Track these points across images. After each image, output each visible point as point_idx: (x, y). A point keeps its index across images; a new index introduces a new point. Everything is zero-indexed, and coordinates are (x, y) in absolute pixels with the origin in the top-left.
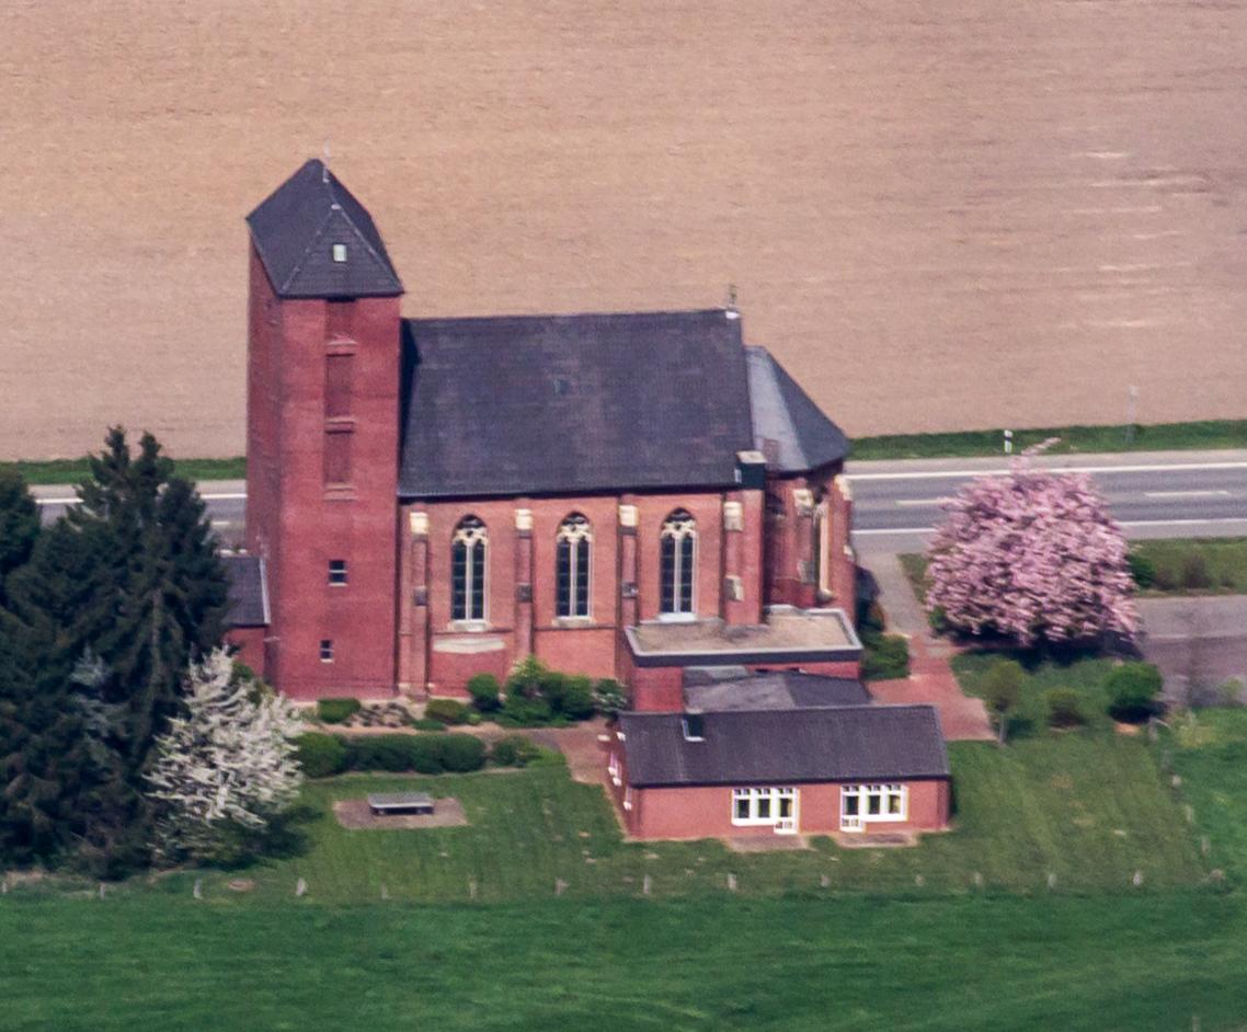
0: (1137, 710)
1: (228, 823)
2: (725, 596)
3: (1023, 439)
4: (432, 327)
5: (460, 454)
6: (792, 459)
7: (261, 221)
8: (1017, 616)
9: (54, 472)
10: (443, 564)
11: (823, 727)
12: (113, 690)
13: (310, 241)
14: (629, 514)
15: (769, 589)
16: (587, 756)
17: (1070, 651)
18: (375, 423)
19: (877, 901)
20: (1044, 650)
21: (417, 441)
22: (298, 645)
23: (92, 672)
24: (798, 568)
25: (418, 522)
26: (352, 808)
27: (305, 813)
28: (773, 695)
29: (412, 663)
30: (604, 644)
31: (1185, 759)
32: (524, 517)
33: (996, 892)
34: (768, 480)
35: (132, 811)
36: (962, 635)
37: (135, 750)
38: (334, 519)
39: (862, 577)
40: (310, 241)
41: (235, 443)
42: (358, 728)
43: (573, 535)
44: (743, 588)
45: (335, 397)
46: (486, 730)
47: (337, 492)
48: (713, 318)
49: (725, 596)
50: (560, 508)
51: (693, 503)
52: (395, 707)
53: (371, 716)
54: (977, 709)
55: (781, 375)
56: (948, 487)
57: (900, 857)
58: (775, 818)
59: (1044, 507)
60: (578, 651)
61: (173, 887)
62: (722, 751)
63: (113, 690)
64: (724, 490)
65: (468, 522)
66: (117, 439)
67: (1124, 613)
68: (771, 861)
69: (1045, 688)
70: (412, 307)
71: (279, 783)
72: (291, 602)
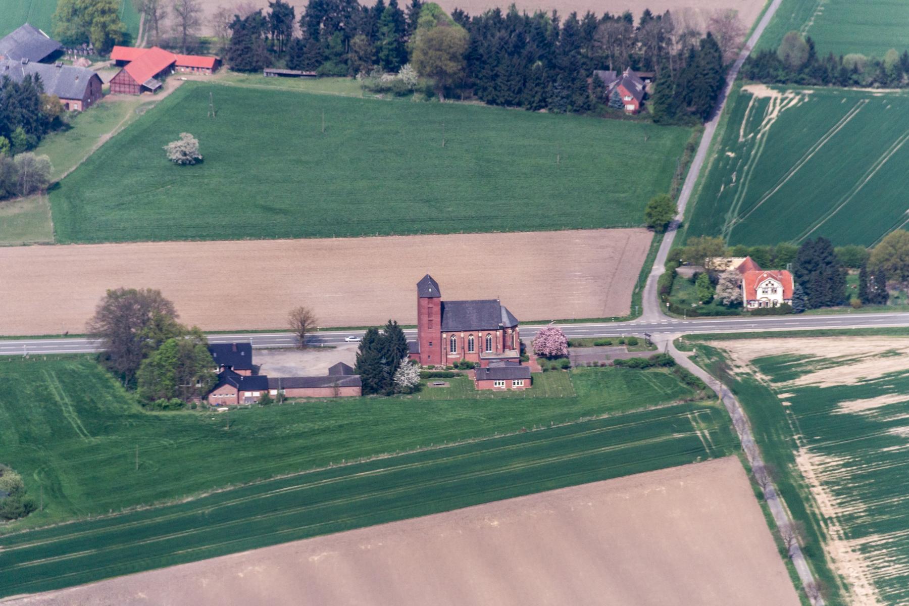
0: (566, 367)
1: (407, 386)
2: (497, 348)
3: (548, 322)
4: (447, 303)
5: (451, 323)
6: (508, 325)
7: (419, 285)
8: (547, 351)
9: (381, 327)
10: (449, 343)
11: (508, 372)
12: (388, 364)
13: (427, 288)
14: (480, 334)
15: (504, 347)
16: (471, 375)
17: (556, 357)
18: (437, 318)
19: (517, 400)
20: (551, 357)
21: (444, 322)
22: (424, 356)
23: (384, 361)
24: (509, 343)
25: (444, 335)
26: (431, 384)
27: (420, 385)
28: (502, 365)
29: (444, 359)
30: (476, 356)
31: (573, 376)
32: (462, 335)
33: (537, 398)
34: (504, 329)
35: (391, 384)
36: (539, 355)
37: (392, 374)
38: (430, 335)
39: (521, 344)
40: (427, 288)
41: (415, 322)
42: (434, 370)
43: (471, 338)
44: (500, 346)
45: (429, 315)
46: (455, 371)
47: (430, 330)
48: (495, 301)
49: (497, 348)
50: (469, 333)
51: (491, 332)
52: (440, 368)
53: (437, 368)
54: (540, 367)
55: (507, 312)
56: (537, 330)
57: (522, 392)
58: (501, 385)
59: (553, 333)
60: (472, 358)
61: (398, 397)
62: (491, 374)
63: (388, 364)
64: (496, 330)
65: (453, 335)
66: (390, 322)
67: (565, 351)
68: (501, 392)
69: (550, 364)
70: (442, 299)
71: (416, 380)
72: (423, 349)
